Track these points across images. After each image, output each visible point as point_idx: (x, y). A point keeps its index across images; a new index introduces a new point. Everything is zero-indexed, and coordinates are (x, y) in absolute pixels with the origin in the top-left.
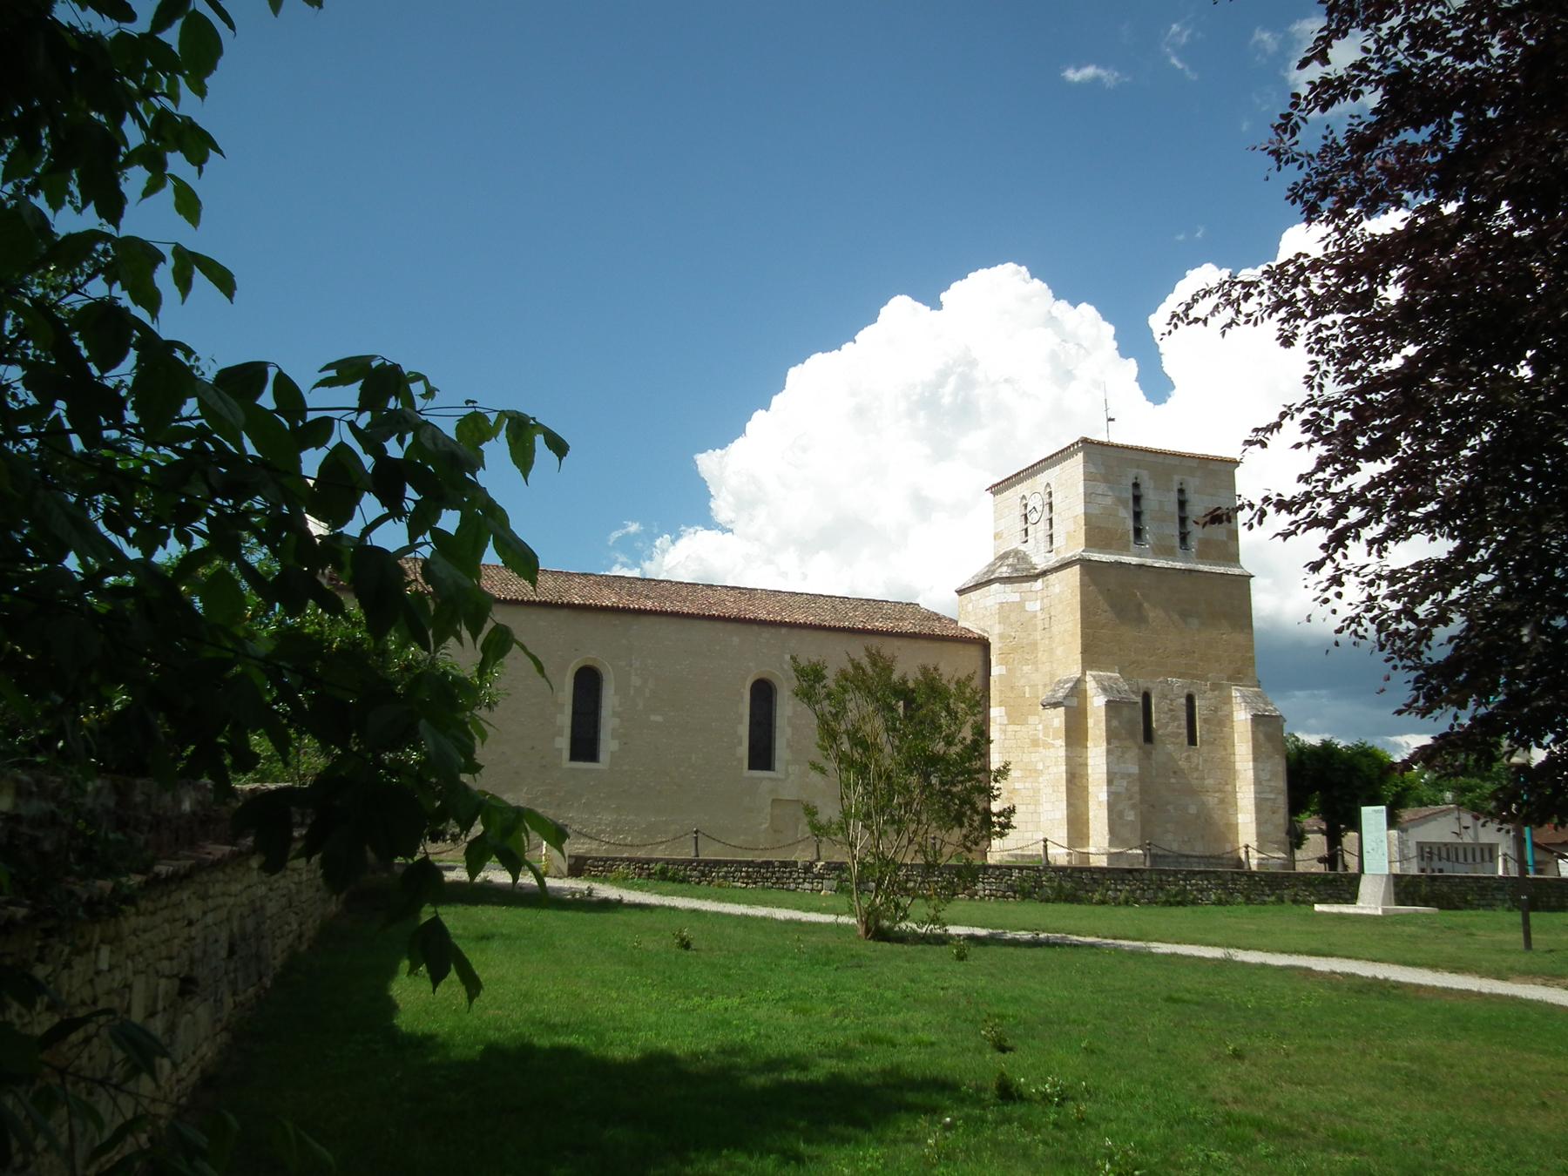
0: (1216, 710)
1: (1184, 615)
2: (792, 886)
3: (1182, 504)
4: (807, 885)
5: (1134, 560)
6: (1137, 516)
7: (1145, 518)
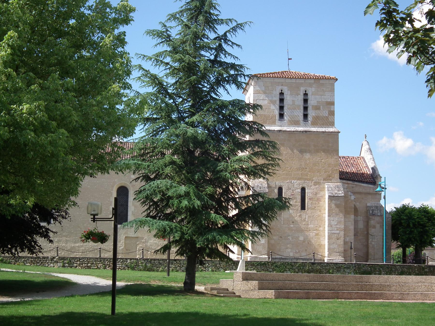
0: (316, 194)
1: (302, 152)
2: (47, 265)
3: (306, 101)
4: (52, 265)
5: (276, 128)
6: (281, 108)
7: (285, 109)
